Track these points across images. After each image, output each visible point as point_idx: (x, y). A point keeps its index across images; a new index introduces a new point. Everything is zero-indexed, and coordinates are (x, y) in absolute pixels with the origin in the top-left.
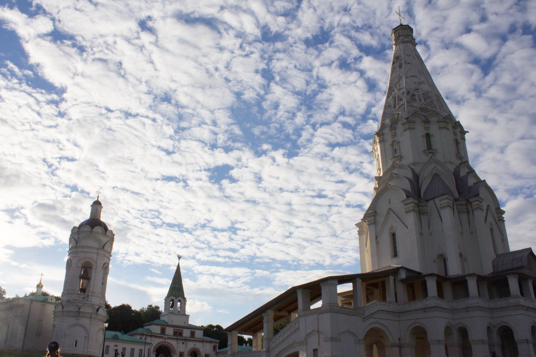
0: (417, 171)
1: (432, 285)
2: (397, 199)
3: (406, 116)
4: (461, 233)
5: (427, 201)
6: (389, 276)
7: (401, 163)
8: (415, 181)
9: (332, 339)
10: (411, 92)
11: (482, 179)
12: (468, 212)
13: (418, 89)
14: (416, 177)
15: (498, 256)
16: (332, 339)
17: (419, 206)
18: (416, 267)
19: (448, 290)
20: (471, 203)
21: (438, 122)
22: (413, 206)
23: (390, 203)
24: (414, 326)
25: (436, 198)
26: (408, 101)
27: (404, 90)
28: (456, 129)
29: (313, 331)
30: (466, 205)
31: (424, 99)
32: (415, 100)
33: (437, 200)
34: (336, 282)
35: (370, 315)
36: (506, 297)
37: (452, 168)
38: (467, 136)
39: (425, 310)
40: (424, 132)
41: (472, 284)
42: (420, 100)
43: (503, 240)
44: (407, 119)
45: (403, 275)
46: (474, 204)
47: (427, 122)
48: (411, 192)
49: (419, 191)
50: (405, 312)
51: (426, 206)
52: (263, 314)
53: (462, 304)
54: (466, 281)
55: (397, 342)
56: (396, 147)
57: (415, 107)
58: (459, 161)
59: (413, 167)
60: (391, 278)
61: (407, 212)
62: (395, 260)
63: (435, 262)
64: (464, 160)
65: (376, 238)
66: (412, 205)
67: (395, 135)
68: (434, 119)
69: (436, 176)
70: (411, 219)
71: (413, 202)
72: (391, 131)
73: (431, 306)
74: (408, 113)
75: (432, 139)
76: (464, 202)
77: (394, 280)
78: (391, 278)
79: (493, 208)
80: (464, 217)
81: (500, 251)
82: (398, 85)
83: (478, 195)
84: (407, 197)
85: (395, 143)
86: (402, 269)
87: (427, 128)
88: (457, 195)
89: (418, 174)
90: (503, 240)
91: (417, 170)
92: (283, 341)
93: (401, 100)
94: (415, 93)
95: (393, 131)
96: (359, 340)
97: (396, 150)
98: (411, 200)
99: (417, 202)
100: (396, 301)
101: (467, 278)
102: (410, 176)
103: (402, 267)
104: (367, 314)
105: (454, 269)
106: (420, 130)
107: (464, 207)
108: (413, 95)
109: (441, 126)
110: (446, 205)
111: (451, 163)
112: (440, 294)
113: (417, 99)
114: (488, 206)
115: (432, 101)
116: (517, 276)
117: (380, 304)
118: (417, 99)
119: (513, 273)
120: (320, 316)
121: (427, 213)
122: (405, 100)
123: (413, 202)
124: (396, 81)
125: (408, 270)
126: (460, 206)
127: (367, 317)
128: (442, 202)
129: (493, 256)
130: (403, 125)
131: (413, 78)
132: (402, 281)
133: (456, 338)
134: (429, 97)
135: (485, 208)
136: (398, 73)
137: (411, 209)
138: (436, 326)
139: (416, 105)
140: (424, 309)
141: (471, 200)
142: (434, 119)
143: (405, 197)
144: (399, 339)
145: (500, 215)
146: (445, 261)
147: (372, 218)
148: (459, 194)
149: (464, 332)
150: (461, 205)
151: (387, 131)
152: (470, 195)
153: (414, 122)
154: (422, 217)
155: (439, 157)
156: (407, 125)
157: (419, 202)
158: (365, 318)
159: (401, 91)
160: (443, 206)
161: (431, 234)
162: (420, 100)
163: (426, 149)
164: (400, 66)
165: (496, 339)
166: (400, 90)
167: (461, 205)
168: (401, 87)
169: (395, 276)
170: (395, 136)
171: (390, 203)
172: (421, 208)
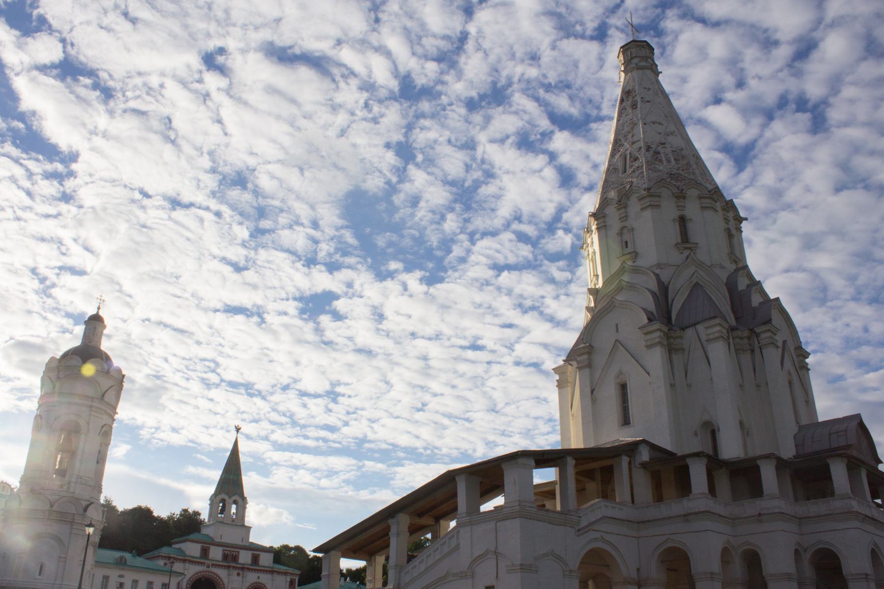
0: (665, 278)
1: (698, 474)
2: (632, 323)
3: (645, 186)
4: (741, 386)
5: (683, 329)
6: (620, 455)
7: (635, 264)
8: (662, 295)
9: (523, 568)
10: (654, 146)
11: (772, 297)
12: (753, 351)
13: (664, 144)
14: (664, 288)
15: (801, 428)
16: (523, 568)
17: (668, 338)
18: (665, 442)
19: (723, 483)
20: (758, 335)
21: (700, 198)
22: (660, 337)
23: (617, 331)
24: (666, 546)
25: (698, 323)
26: (647, 162)
27: (642, 144)
28: (728, 212)
29: (487, 552)
30: (749, 338)
32: (661, 161)
33: (700, 327)
34: (533, 463)
35: (590, 524)
36: (824, 496)
37: (724, 276)
38: (744, 224)
39: (686, 517)
40: (676, 214)
41: (768, 474)
42: (669, 161)
43: (807, 402)
44: (649, 189)
45: (645, 455)
46: (763, 336)
47: (680, 196)
48: (655, 313)
49: (669, 313)
50: (649, 521)
51: (681, 337)
52: (390, 521)
53: (750, 507)
54: (757, 468)
55: (634, 575)
56: (627, 237)
57: (660, 171)
58: (734, 267)
59: (657, 271)
60: (625, 460)
61: (649, 347)
62: (626, 430)
63: (696, 434)
64: (740, 265)
65: (592, 391)
66: (658, 334)
67: (626, 216)
68: (693, 193)
69: (696, 286)
70: (656, 358)
71: (660, 330)
72: (618, 210)
73: (697, 510)
74: (649, 180)
75: (690, 225)
76: (746, 333)
77: (630, 463)
78: (625, 460)
79: (791, 346)
80: (746, 358)
81: (804, 421)
82: (630, 136)
83: (769, 321)
84: (650, 320)
85: (625, 231)
86: (643, 445)
87: (680, 207)
88: (733, 322)
89: (666, 283)
90: (807, 402)
91: (665, 276)
92: (427, 569)
93: (636, 159)
94: (659, 149)
95: (623, 210)
96: (571, 571)
97: (626, 242)
98: (656, 325)
99: (665, 329)
100: (633, 502)
101: (759, 462)
102: (653, 285)
103: (644, 441)
104: (584, 523)
105: (731, 448)
106: (669, 210)
107: (746, 341)
108: (657, 153)
109: (704, 205)
110: (717, 335)
111: (722, 267)
112: (712, 490)
113: (664, 159)
114: (784, 342)
115: (688, 164)
116: (846, 460)
117: (606, 506)
118: (664, 159)
119: (840, 456)
120: (499, 524)
121: (684, 350)
122: (642, 160)
123: (660, 330)
124: (626, 129)
125: (653, 447)
126: (738, 340)
127: (584, 528)
128: (710, 331)
129: (793, 429)
130: (640, 200)
131: (656, 125)
132: (644, 465)
133: (738, 569)
134: (683, 157)
135: (780, 344)
136: (630, 117)
137: (657, 340)
138: (706, 547)
139: (661, 168)
140: (685, 515)
141: (757, 330)
142: (693, 193)
143: (646, 321)
144: (638, 569)
145: (801, 358)
146: (713, 433)
147: (585, 357)
148: (737, 319)
149: (753, 560)
150: (741, 338)
151: (611, 210)
152: (754, 321)
153: (659, 196)
154: (674, 356)
156: (647, 200)
157: (669, 330)
158: (581, 531)
159: (636, 146)
160: (711, 337)
161: (689, 386)
162: (669, 161)
163: (680, 241)
164: (634, 106)
165: (809, 572)
166: (633, 143)
167: (741, 338)
168: (635, 139)
169: (630, 457)
171: (617, 331)
172: (672, 340)
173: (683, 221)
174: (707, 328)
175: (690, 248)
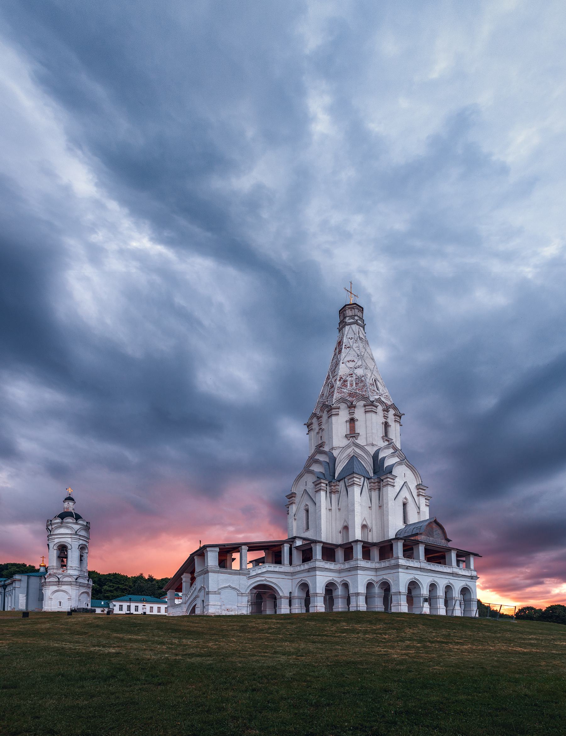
13: (352, 374)
31: (356, 384)
37: (372, 451)
40: (347, 417)
42: (352, 385)
45: (299, 543)
47: (352, 406)
57: (344, 392)
69: (353, 459)
80: (375, 494)
126: (372, 484)
132: (297, 548)
134: (362, 381)
139: (345, 390)
144: (290, 593)
150: (374, 483)
155: (361, 441)
162: (352, 385)
170: (320, 424)
173: (352, 421)
174: (349, 479)
175: (354, 436)
